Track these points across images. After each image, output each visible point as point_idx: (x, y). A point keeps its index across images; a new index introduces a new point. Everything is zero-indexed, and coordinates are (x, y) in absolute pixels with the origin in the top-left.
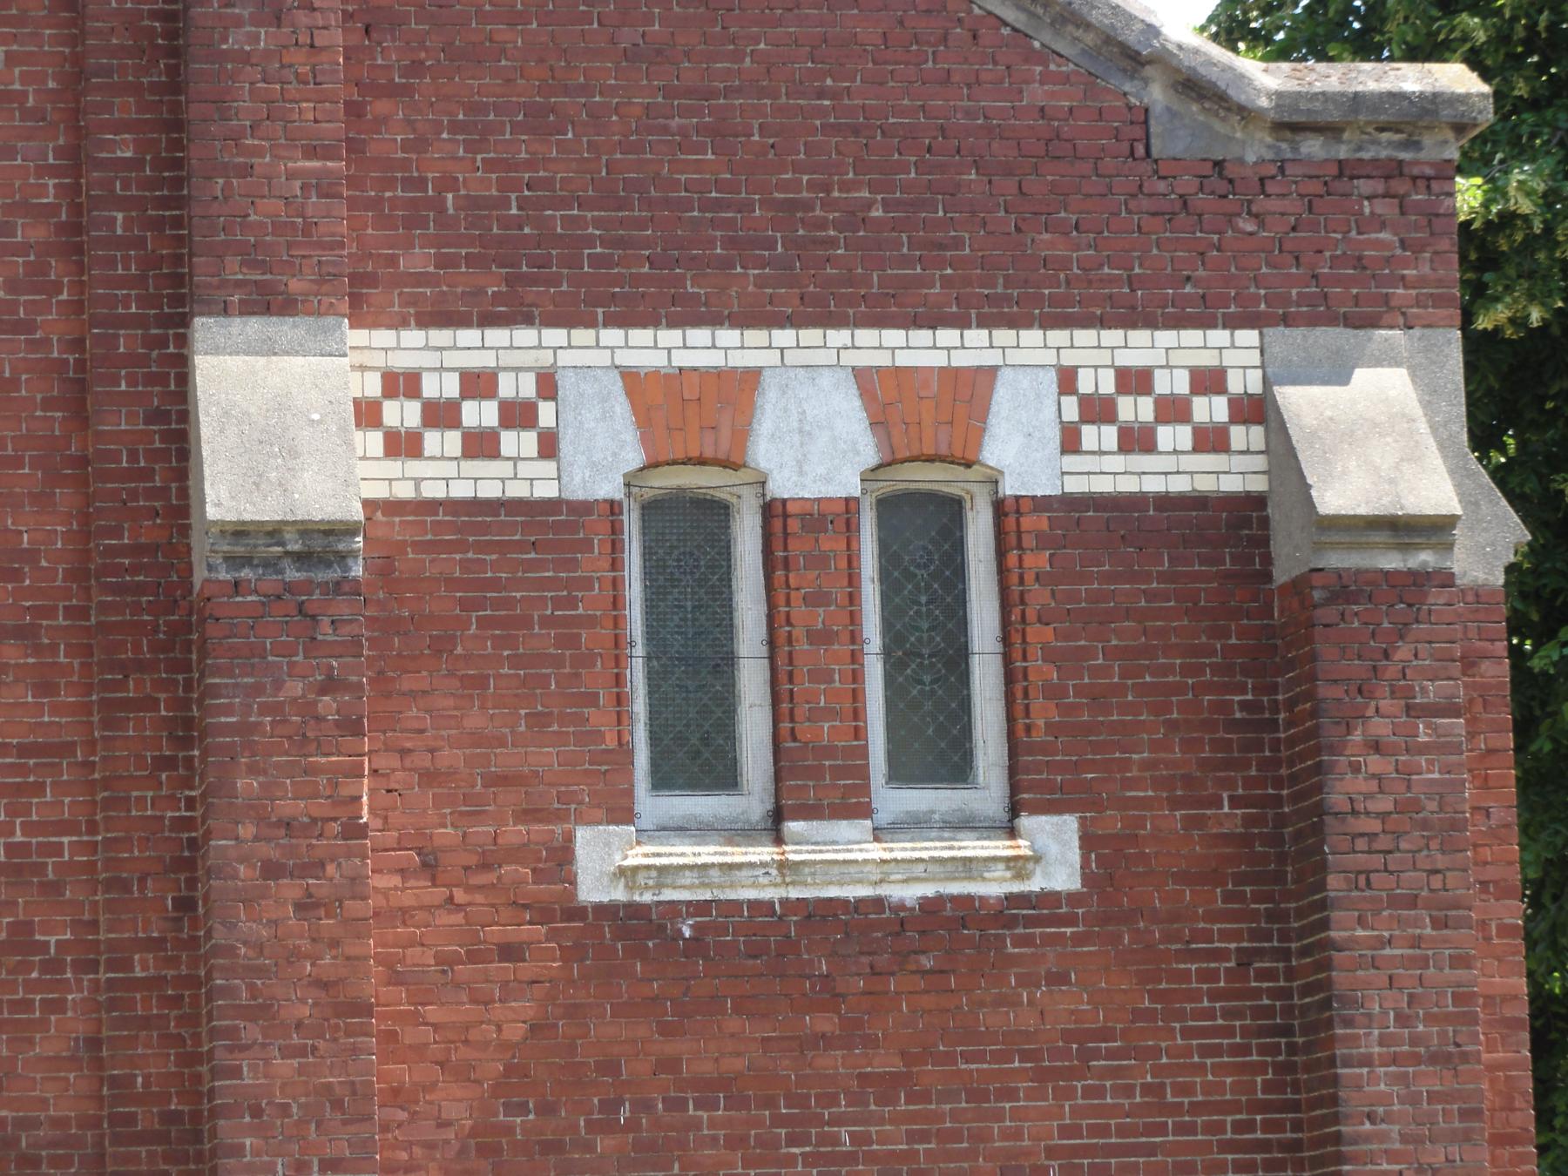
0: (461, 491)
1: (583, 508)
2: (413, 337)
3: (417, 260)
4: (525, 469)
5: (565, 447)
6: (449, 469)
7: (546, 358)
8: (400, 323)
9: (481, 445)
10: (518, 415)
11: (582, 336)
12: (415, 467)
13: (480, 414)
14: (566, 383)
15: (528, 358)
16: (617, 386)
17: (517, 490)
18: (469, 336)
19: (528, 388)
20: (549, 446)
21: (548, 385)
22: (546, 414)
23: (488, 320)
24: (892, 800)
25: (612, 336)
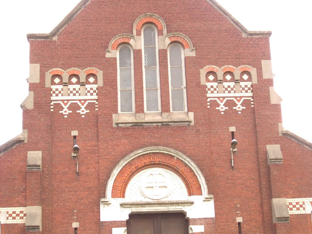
0: (297, 213)
1: (307, 215)
2: (291, 199)
3: (291, 192)
4: (302, 211)
5: (306, 209)
6: (295, 211)
7: (303, 201)
8: (290, 198)
9: (298, 209)
10: (301, 206)
11: (306, 199)
12: (292, 211)
13: (298, 206)
14: (305, 203)
15: (302, 201)
16: (310, 203)
17: (302, 213)
18: (296, 199)
19: (302, 204)
20: (304, 209)
21: (304, 203)
22: (304, 206)
23: (298, 198)
25: (309, 198)
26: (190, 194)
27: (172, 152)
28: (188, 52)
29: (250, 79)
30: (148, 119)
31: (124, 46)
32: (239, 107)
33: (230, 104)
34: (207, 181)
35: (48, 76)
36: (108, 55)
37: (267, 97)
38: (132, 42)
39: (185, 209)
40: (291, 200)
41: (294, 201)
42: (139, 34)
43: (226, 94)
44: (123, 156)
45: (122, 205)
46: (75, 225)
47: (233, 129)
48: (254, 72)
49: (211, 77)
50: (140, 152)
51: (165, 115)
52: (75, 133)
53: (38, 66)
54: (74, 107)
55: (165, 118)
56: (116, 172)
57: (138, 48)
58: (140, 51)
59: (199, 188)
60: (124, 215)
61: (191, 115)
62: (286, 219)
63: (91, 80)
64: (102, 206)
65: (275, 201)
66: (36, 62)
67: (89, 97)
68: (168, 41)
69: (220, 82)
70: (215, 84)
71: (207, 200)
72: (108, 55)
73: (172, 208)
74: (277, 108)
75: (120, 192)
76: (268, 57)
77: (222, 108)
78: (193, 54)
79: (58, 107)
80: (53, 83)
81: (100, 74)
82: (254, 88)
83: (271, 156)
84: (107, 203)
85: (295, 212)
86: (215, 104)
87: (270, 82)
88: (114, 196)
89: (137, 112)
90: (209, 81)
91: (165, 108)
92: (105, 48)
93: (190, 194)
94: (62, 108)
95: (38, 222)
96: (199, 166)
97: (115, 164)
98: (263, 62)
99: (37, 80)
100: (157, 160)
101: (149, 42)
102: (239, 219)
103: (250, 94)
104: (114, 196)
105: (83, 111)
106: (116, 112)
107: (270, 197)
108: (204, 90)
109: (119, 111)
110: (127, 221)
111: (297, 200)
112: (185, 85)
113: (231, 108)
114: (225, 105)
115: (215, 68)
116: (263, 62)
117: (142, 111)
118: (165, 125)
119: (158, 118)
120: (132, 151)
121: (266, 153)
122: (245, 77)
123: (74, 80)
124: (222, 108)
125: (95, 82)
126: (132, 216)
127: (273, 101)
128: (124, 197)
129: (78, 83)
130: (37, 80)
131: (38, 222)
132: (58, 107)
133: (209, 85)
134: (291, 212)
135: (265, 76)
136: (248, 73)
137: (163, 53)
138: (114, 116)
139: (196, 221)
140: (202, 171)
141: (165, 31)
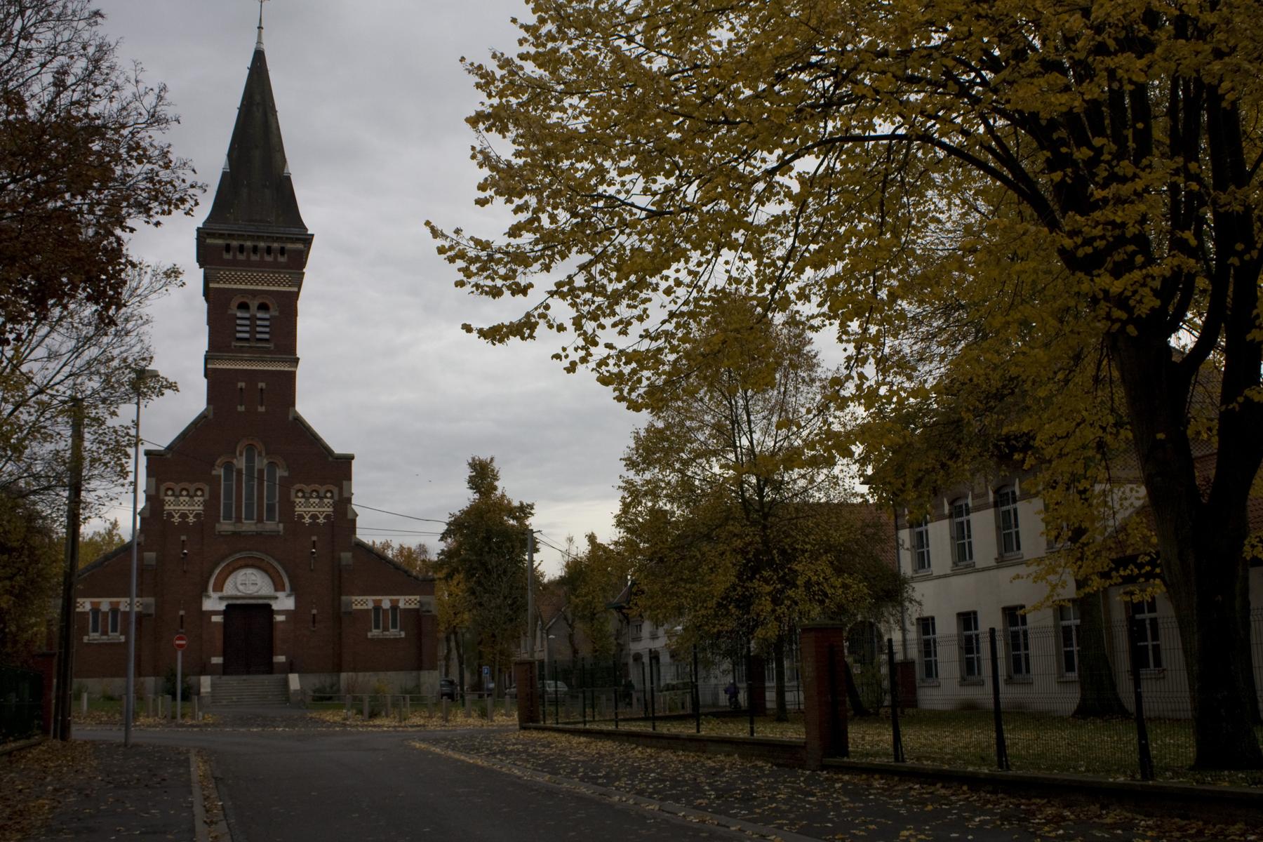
24: (391, 630)
26: (276, 590)
27: (264, 556)
28: (281, 473)
29: (332, 497)
30: (244, 529)
31: (228, 467)
32: (321, 520)
33: (314, 517)
34: (290, 581)
35: (163, 488)
36: (214, 472)
37: (345, 514)
38: (235, 461)
39: (272, 602)
40: (357, 598)
41: (359, 598)
42: (241, 455)
43: (312, 509)
44: (223, 559)
45: (221, 598)
46: (182, 613)
47: (314, 538)
48: (336, 491)
49: (300, 494)
50: (238, 556)
51: (259, 525)
52: (183, 538)
53: (153, 480)
54: (184, 516)
55: (259, 528)
56: (217, 572)
57: (239, 467)
58: (241, 470)
59: (284, 586)
60: (222, 606)
61: (281, 526)
62: (350, 613)
63: (199, 493)
64: (204, 599)
65: (344, 598)
66: (153, 476)
67: (197, 508)
68: (265, 461)
69: (307, 499)
70: (303, 500)
71: (289, 596)
72: (214, 472)
73: (261, 602)
74: (352, 523)
75: (219, 587)
76: (350, 479)
77: (307, 520)
78: (286, 474)
79: (170, 515)
80: (166, 495)
81: (207, 489)
82: (335, 505)
83: (344, 562)
84: (209, 597)
85: (359, 607)
86: (301, 517)
87: (349, 500)
88: (214, 591)
89: (236, 522)
90: (298, 497)
91: (260, 520)
92: (212, 466)
93: (276, 590)
94: (173, 517)
95: (152, 610)
96: (284, 568)
97: (216, 565)
98: (345, 483)
99: (153, 492)
100: (250, 562)
101: (250, 460)
102: (314, 611)
103: (331, 509)
104: (214, 590)
105: (191, 519)
106: (218, 521)
107: (341, 595)
108: (293, 504)
109: (222, 520)
110: (224, 611)
111: (361, 598)
112: (277, 499)
113: (314, 520)
114: (310, 518)
115: (303, 486)
116: (345, 483)
117: (241, 522)
118: (259, 534)
119: (253, 528)
120: (230, 555)
121: (340, 559)
122: (329, 495)
123: (184, 493)
124: (307, 520)
125: (202, 496)
126: (228, 606)
127: (350, 516)
128: (222, 591)
129: (187, 495)
130: (153, 492)
131: (152, 610)
132: (170, 515)
133: (297, 500)
134: (354, 607)
135: (346, 495)
136: (331, 492)
137: (261, 472)
138: (217, 525)
139: (280, 612)
140: (286, 572)
141: (264, 454)
